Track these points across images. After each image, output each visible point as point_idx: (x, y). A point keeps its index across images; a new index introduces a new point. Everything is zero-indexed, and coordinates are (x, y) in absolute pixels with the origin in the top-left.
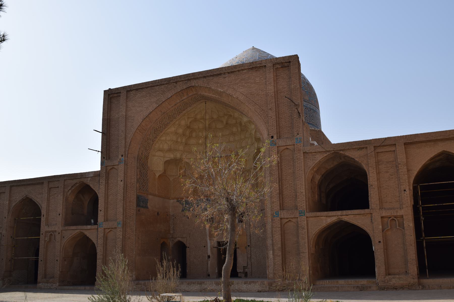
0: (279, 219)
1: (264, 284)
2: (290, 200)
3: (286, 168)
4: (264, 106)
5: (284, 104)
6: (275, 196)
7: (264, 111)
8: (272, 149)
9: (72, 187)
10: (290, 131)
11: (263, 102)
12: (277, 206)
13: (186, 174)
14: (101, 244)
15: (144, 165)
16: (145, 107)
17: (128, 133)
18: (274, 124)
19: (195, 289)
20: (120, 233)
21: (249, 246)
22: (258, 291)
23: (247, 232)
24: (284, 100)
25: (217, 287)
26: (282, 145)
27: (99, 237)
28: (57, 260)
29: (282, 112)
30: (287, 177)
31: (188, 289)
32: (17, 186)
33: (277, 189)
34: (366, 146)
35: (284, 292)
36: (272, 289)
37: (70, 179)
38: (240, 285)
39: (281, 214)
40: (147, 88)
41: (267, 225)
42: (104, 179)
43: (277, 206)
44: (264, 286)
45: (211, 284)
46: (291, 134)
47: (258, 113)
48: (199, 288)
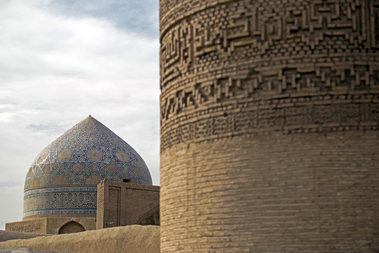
16: (141, 208)
40: (142, 190)
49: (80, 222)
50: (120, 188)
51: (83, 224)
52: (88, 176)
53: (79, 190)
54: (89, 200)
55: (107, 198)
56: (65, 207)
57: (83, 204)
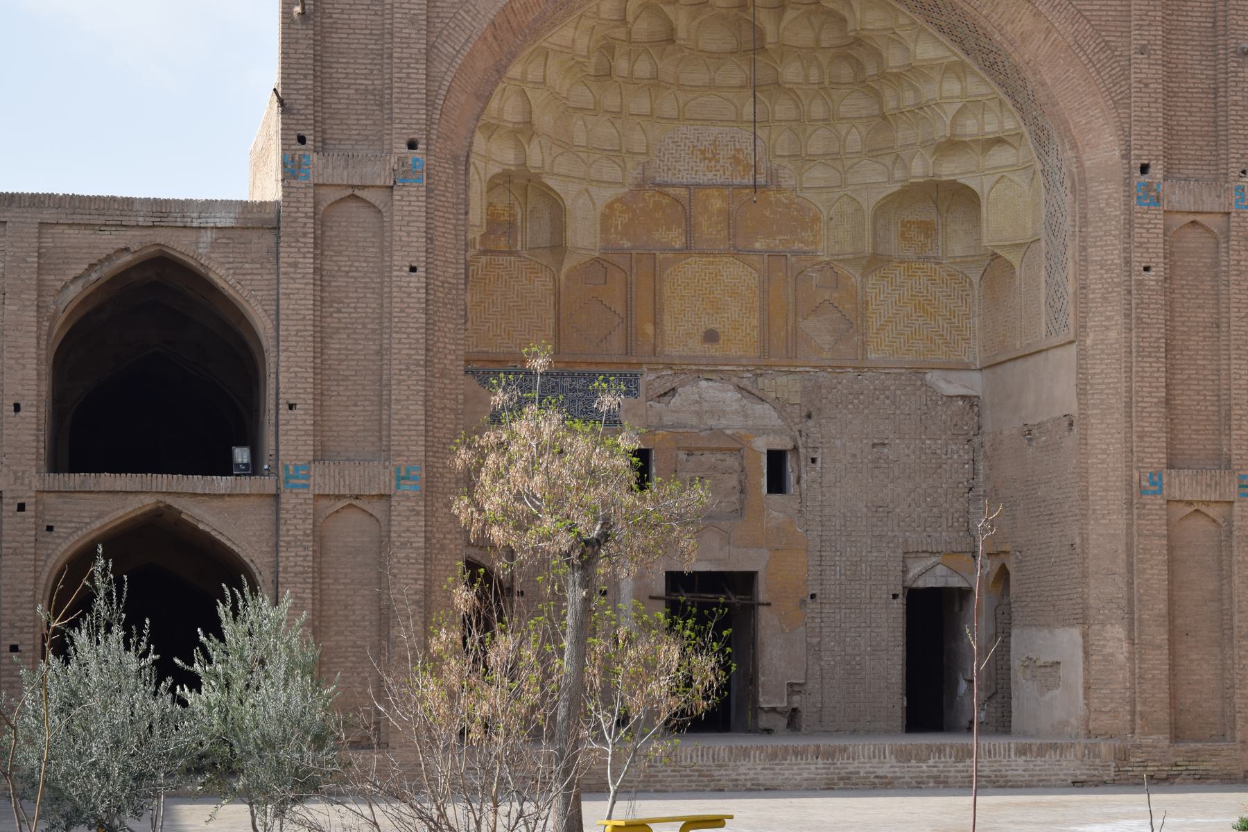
0: (1161, 502)
1: (1099, 756)
2: (1194, 430)
3: (1185, 300)
4: (1114, 29)
5: (1187, 37)
6: (1151, 413)
7: (1113, 52)
8: (1142, 218)
9: (92, 266)
10: (1205, 153)
11: (1110, 13)
12: (1155, 453)
13: (519, 248)
17: (441, 32)
18: (1153, 115)
19: (805, 775)
21: (813, 596)
22: (1073, 783)
23: (810, 538)
24: (1190, 19)
25: (903, 767)
26: (1183, 209)
27: (287, 539)
29: (1177, 67)
30: (1190, 340)
31: (773, 779)
33: (1160, 384)
35: (1172, 784)
36: (1130, 774)
37: (79, 224)
38: (1002, 758)
39: (1170, 486)
41: (1087, 524)
43: (1155, 453)
44: (1098, 761)
45: (874, 757)
46: (1209, 165)
47: (1087, 56)
48: (824, 771)
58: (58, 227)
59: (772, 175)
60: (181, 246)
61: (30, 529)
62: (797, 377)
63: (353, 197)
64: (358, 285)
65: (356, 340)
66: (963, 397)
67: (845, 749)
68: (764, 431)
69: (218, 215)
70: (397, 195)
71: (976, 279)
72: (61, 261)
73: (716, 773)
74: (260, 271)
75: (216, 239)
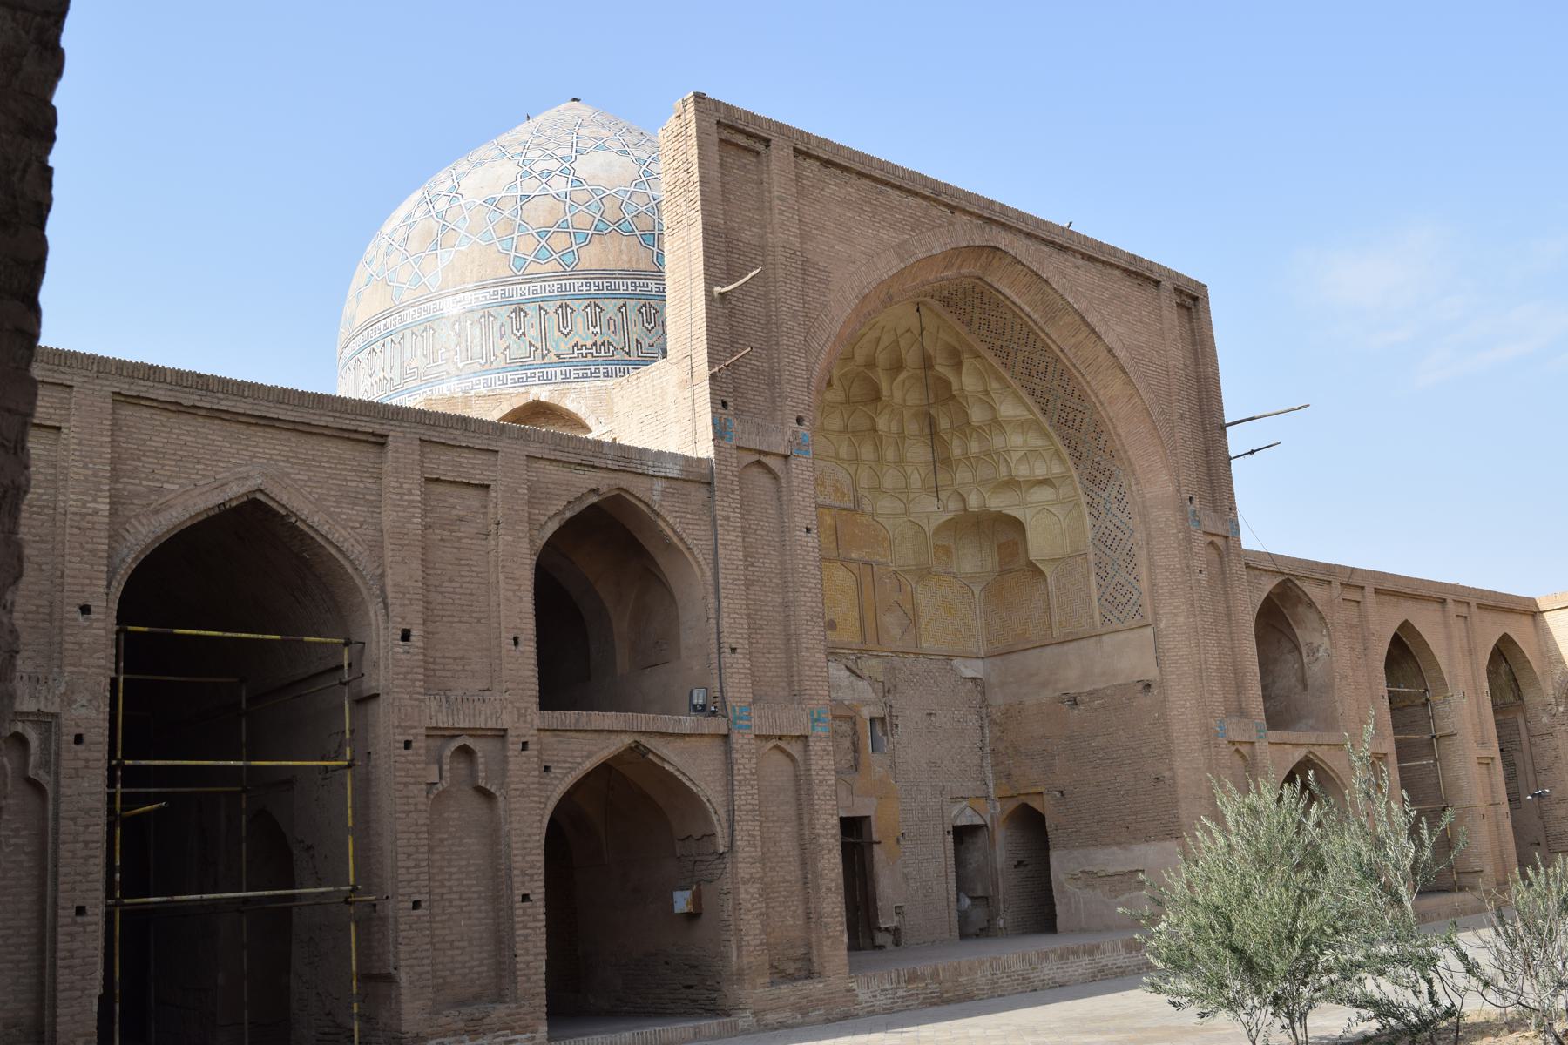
14: (750, 807)
15: (1124, 502)
16: (862, 252)
19: (1080, 971)
20: (826, 762)
28: (525, 898)
32: (162, 406)
34: (1330, 578)
40: (861, 175)
42: (734, 505)
49: (567, 402)
50: (767, 142)
51: (583, 408)
52: (588, 239)
53: (556, 293)
54: (598, 329)
55: (711, 173)
56: (503, 364)
57: (576, 344)
58: (541, 462)
59: (857, 501)
60: (638, 488)
61: (535, 770)
62: (880, 660)
63: (759, 463)
64: (764, 542)
65: (766, 592)
66: (973, 679)
67: (1098, 947)
68: (865, 703)
69: (668, 466)
70: (793, 462)
71: (977, 590)
72: (543, 496)
73: (1032, 976)
74: (699, 522)
75: (666, 488)
